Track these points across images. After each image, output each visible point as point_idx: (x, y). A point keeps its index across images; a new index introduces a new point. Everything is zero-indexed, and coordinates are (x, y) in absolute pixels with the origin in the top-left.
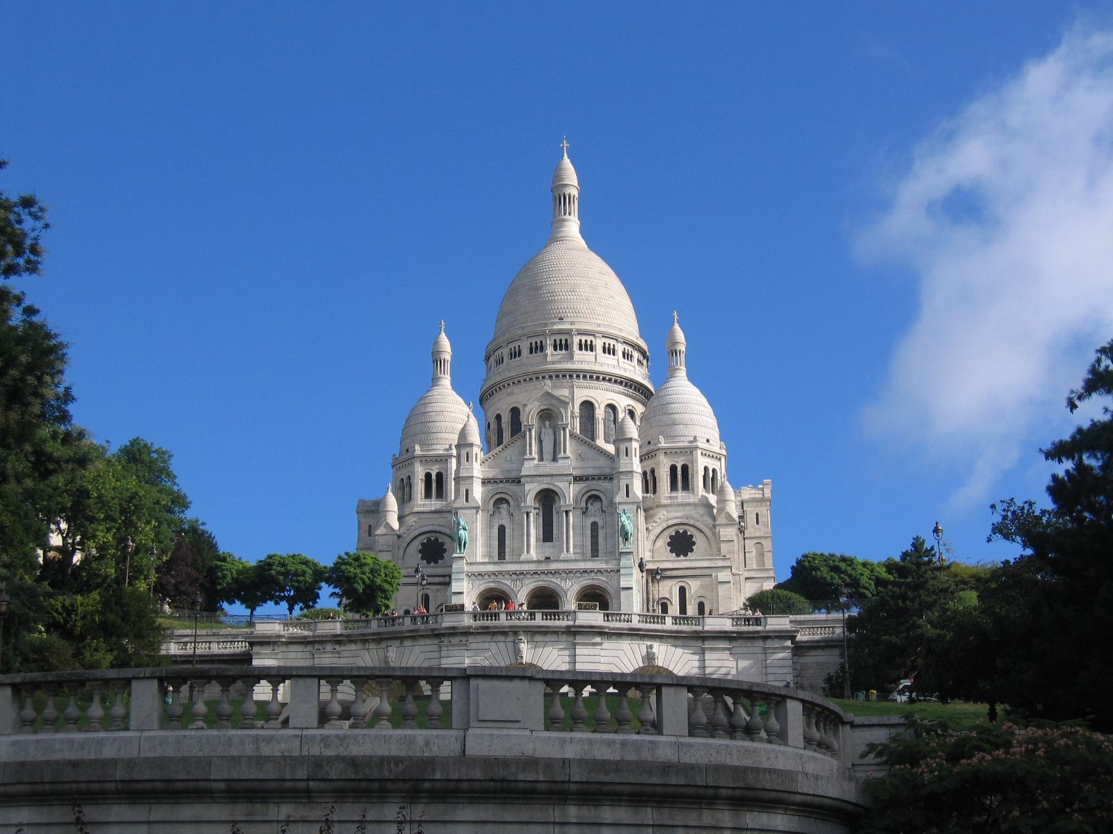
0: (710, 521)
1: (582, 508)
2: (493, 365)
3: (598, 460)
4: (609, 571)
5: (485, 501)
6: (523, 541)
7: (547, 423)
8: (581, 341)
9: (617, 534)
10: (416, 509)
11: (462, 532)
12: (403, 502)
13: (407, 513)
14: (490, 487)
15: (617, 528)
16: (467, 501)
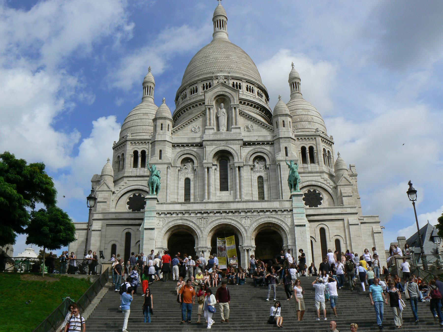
0: (332, 183)
1: (250, 166)
2: (180, 101)
3: (262, 131)
4: (283, 210)
5: (175, 160)
6: (204, 190)
7: (222, 104)
8: (233, 83)
9: (280, 184)
10: (126, 175)
11: (155, 178)
12: (119, 171)
13: (120, 177)
14: (178, 150)
15: (280, 180)
16: (160, 158)
